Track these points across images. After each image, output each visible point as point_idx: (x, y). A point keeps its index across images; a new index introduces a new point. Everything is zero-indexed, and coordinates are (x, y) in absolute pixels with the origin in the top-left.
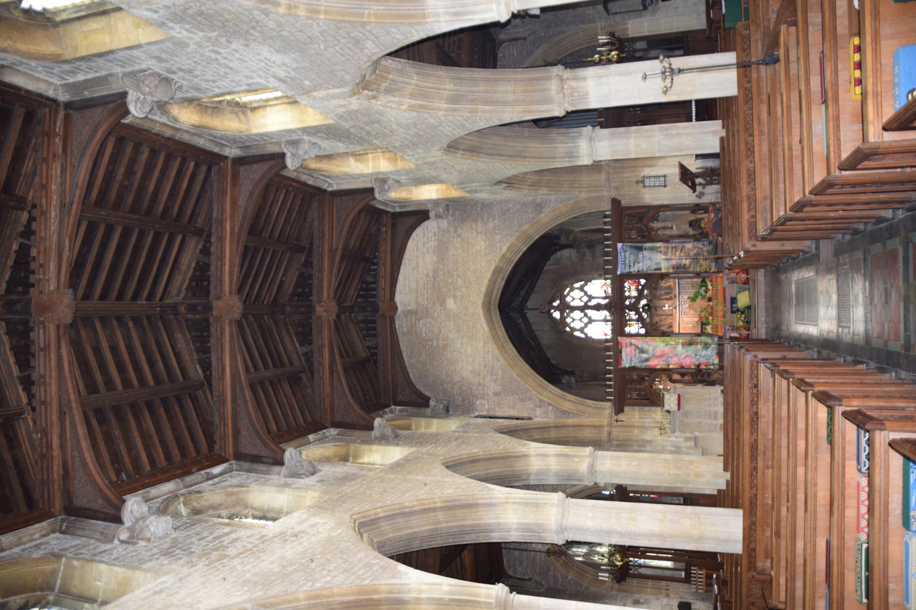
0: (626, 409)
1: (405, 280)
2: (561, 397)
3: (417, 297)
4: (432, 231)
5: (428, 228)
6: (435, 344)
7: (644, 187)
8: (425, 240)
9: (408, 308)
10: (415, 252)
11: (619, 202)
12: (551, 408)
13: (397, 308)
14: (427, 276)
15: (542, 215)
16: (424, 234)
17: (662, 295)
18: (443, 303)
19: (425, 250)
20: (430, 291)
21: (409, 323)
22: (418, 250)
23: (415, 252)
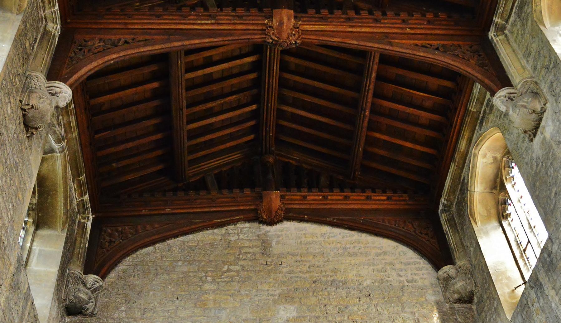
1: (322, 235)
3: (293, 255)
4: (416, 277)
5: (421, 269)
6: (207, 287)
8: (398, 266)
9: (274, 243)
10: (374, 251)
13: (271, 223)
14: (335, 271)
16: (409, 264)
18: (287, 298)
19: (380, 267)
20: (308, 275)
21: (247, 244)
22: (378, 255)
23: (374, 251)
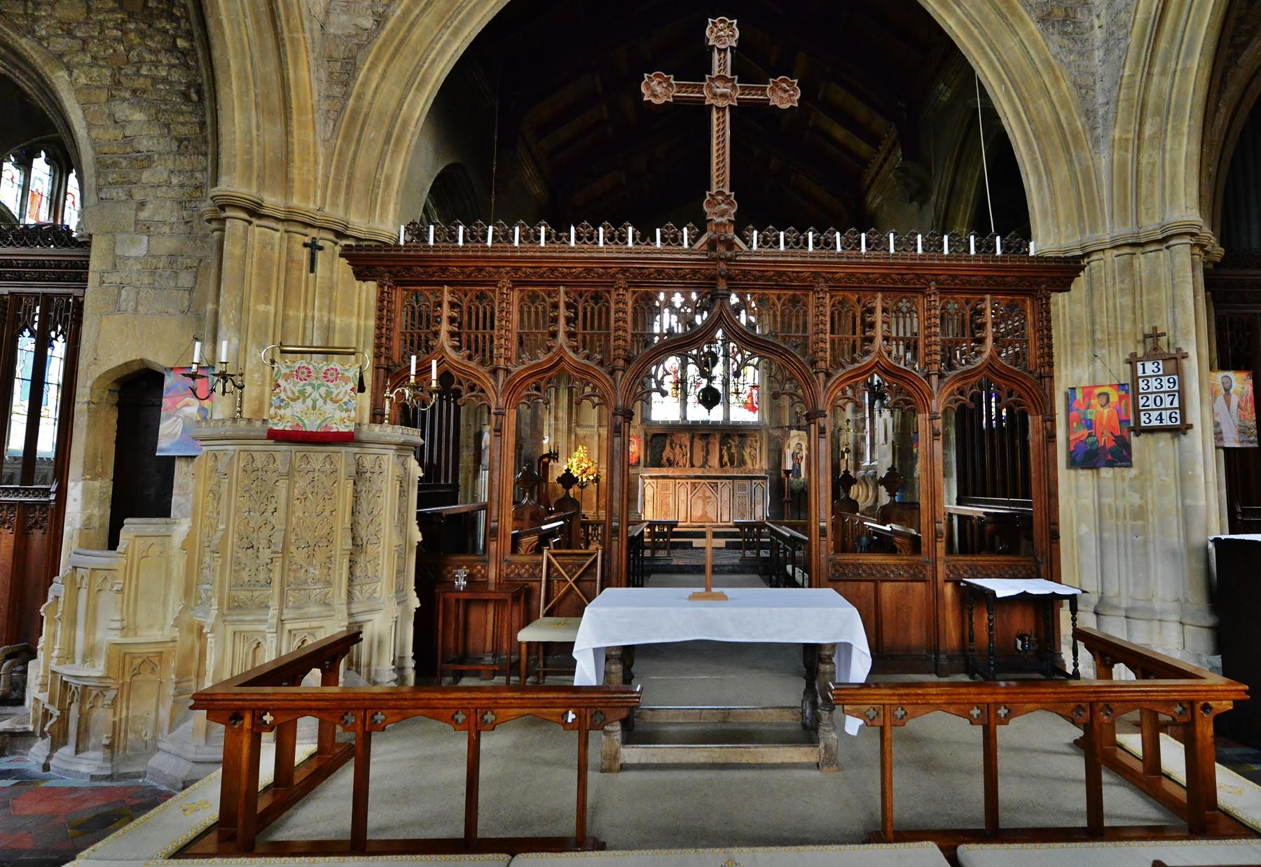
0: (370, 289)
2: (415, 73)
7: (1132, 361)
11: (1065, 287)
12: (368, 23)
15: (1034, 27)
17: (729, 449)
